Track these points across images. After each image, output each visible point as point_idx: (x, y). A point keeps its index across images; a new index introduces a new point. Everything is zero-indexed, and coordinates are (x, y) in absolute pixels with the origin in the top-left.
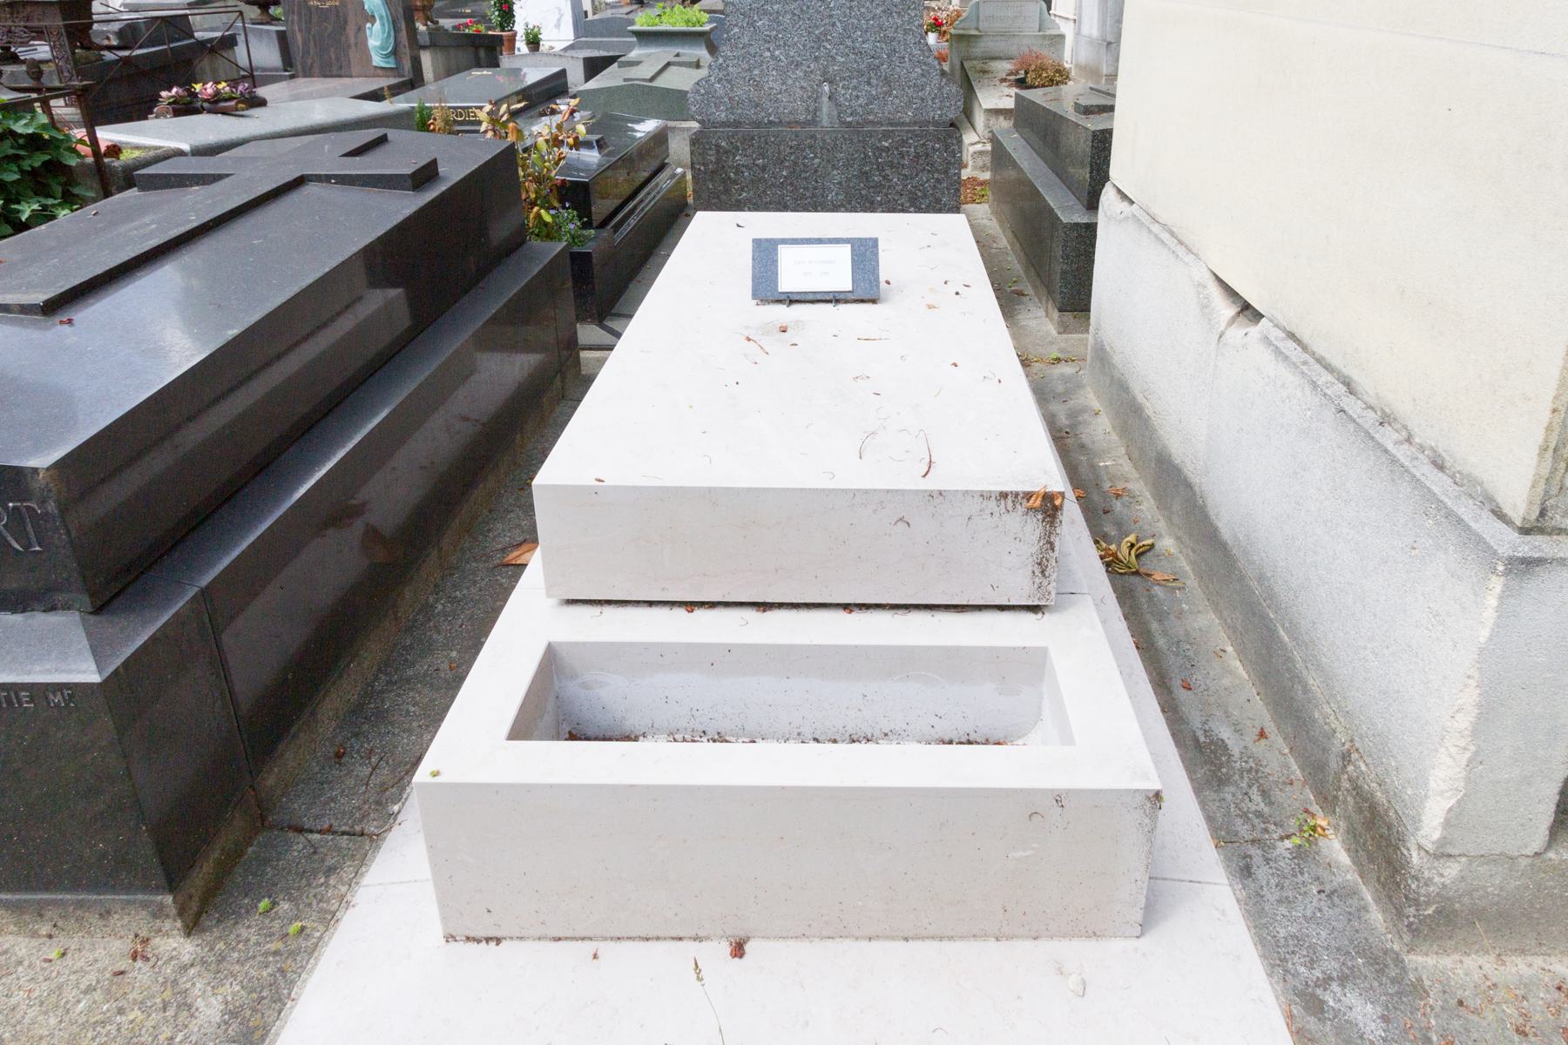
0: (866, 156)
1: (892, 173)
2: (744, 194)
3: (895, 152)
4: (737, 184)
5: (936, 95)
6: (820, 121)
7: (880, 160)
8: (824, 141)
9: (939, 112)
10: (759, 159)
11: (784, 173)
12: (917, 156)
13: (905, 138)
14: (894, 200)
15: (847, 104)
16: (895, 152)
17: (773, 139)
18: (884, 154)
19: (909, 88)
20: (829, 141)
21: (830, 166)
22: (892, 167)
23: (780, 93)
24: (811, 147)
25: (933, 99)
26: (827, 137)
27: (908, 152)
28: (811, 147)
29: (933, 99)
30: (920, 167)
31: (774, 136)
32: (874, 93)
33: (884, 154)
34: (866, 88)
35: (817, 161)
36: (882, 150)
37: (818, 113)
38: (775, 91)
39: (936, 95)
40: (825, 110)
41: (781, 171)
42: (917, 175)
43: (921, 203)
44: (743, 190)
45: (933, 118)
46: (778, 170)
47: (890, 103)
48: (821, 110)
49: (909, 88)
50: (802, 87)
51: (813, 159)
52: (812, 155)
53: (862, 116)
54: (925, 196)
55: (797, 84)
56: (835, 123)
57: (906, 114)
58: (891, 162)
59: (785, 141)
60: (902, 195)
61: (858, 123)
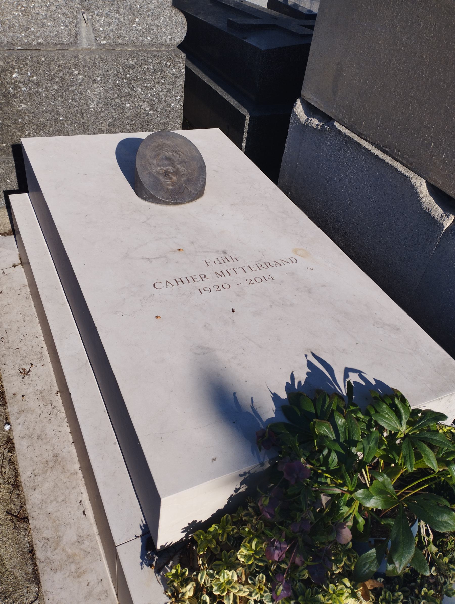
0: (118, 72)
1: (137, 85)
2: (23, 106)
3: (140, 69)
4: (16, 98)
5: (167, 23)
6: (81, 44)
7: (128, 75)
8: (85, 60)
9: (169, 37)
10: (33, 76)
11: (55, 87)
12: (155, 72)
13: (146, 58)
14: (139, 105)
15: (101, 29)
16: (140, 69)
17: (43, 59)
18: (131, 71)
19: (148, 16)
20: (89, 60)
21: (91, 81)
22: (137, 81)
23: (46, 18)
24: (75, 65)
25: (166, 26)
26: (87, 58)
27: (148, 69)
28: (75, 65)
29: (166, 26)
30: (156, 81)
31: (44, 57)
32: (122, 20)
33: (131, 71)
34: (117, 16)
35: (81, 76)
36: (129, 68)
37: (78, 37)
38: (41, 17)
39: (167, 23)
40: (84, 33)
41: (52, 86)
42: (155, 87)
43: (157, 108)
44: (21, 102)
45: (166, 42)
46: (49, 85)
47: (134, 29)
48: (80, 34)
49: (148, 16)
50: (64, 14)
51: (77, 75)
52: (76, 72)
53: (113, 39)
54: (160, 102)
55: (60, 10)
56: (93, 45)
57: (146, 38)
58: (137, 77)
59: (53, 60)
60: (144, 102)
61: (110, 45)
